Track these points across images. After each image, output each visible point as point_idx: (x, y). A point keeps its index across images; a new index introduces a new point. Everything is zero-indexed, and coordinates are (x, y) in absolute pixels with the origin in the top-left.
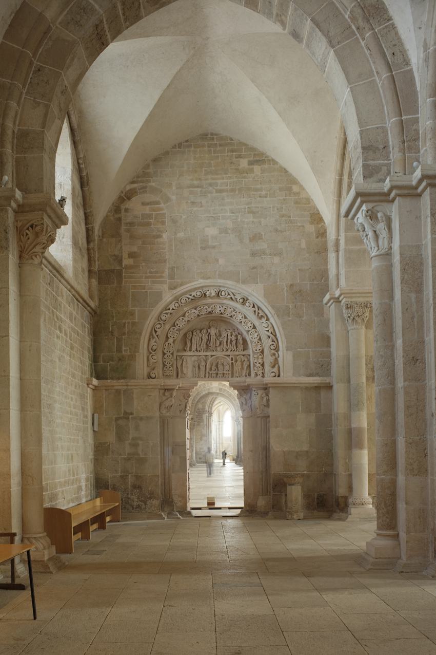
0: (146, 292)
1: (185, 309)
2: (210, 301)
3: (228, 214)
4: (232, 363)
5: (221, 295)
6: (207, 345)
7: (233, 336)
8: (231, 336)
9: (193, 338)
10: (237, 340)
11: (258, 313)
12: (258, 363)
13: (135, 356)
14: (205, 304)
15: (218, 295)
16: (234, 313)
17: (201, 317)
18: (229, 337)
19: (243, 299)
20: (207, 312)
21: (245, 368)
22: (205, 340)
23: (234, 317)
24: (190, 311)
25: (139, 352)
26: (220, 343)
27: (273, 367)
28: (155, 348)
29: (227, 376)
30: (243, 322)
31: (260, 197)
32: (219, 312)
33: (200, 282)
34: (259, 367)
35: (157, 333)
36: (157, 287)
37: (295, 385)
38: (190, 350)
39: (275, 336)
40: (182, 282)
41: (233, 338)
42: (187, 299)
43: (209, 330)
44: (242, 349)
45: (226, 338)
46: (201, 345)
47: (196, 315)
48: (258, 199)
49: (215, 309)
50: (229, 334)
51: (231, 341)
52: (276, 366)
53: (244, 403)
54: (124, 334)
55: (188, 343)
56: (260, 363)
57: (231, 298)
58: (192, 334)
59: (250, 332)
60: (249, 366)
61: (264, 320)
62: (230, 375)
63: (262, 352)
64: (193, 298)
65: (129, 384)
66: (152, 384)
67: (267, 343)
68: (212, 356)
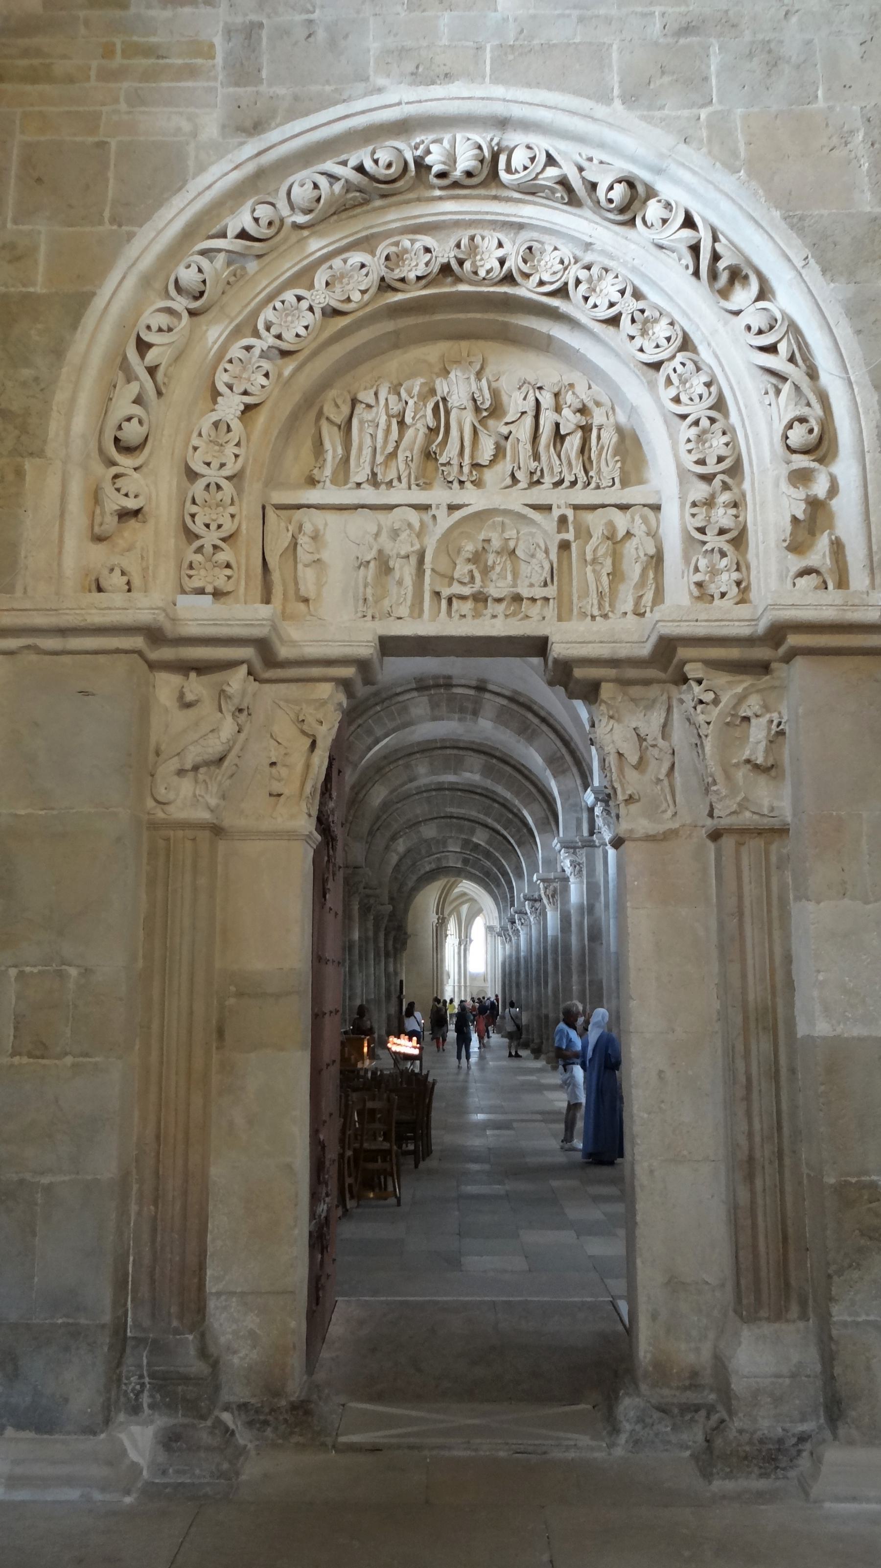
0: (102, 145)
4: (565, 546)
5: (508, 169)
6: (429, 455)
7: (566, 412)
8: (558, 409)
10: (586, 430)
11: (716, 257)
13: (20, 473)
16: (575, 271)
17: (399, 297)
18: (547, 419)
19: (631, 185)
20: (436, 269)
21: (634, 571)
22: (415, 435)
23: (577, 295)
24: (337, 262)
25: (39, 453)
26: (499, 452)
28: (132, 432)
29: (535, 611)
30: (625, 321)
32: (498, 273)
35: (152, 356)
39: (813, 374)
40: (296, 98)
41: (569, 420)
42: (323, 182)
43: (442, 387)
44: (617, 475)
45: (529, 420)
46: (393, 455)
47: (374, 278)
49: (473, 248)
50: (546, 400)
51: (559, 437)
52: (823, 542)
53: (633, 759)
55: (327, 445)
56: (722, 532)
57: (564, 182)
58: (354, 402)
59: (667, 369)
60: (657, 560)
61: (742, 297)
63: (736, 470)
66: (97, 618)
68: (452, 508)
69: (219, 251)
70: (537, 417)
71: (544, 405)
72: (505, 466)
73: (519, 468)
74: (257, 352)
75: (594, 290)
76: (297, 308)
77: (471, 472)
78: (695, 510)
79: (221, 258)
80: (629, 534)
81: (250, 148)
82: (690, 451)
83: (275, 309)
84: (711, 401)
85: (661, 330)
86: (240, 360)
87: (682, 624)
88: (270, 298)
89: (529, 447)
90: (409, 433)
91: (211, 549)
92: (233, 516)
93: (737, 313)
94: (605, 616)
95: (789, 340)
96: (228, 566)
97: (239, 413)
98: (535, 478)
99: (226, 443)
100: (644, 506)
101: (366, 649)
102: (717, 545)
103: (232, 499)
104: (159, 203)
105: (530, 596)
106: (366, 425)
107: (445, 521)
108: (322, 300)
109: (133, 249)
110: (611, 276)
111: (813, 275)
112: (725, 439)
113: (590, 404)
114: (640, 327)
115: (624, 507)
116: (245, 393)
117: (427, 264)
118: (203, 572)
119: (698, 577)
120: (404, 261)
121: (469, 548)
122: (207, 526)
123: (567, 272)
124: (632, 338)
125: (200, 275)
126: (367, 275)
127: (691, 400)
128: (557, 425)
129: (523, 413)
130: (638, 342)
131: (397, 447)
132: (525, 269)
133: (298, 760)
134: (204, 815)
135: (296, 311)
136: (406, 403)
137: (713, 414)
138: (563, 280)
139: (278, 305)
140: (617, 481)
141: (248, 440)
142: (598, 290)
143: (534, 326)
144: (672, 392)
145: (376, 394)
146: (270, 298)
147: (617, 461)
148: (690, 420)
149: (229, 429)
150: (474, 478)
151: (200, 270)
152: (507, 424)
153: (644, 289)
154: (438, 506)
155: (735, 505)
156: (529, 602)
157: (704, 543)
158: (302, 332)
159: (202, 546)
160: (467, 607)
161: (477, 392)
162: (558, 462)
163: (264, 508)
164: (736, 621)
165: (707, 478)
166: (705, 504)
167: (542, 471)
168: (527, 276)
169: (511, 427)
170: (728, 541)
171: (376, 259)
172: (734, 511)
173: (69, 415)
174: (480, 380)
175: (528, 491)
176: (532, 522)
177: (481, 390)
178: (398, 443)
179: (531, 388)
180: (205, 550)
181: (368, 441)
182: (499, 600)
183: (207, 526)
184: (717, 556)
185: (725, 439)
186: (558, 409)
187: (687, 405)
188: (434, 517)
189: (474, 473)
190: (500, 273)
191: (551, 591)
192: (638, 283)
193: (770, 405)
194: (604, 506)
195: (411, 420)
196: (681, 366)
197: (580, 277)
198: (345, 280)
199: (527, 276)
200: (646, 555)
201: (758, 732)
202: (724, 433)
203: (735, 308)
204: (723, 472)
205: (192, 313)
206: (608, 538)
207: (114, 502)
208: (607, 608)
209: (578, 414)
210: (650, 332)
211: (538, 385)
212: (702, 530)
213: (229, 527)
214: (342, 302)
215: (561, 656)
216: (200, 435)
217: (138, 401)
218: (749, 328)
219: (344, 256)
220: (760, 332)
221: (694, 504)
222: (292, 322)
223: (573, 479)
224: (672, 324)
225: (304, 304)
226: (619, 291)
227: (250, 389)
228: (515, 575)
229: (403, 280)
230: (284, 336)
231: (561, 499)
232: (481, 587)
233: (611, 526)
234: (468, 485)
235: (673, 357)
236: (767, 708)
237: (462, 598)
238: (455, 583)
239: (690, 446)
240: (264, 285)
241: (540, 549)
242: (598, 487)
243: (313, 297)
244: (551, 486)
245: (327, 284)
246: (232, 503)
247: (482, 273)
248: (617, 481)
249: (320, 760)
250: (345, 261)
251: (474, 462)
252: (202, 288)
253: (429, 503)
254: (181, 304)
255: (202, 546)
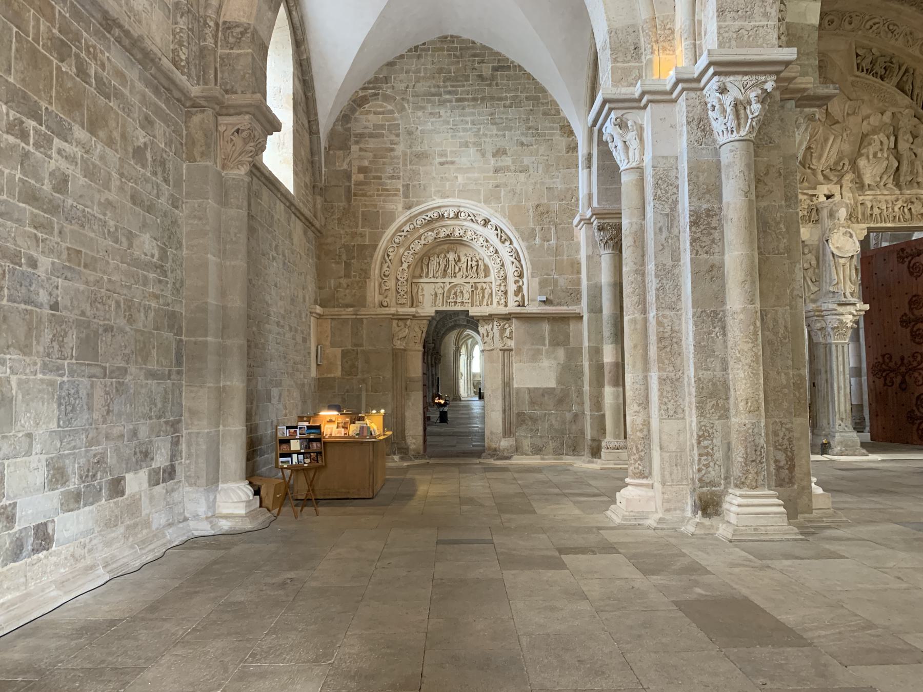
1: (422, 231)
2: (449, 222)
3: (470, 126)
4: (472, 291)
10: (478, 265)
11: (501, 236)
13: (366, 282)
14: (443, 226)
15: (457, 216)
18: (470, 263)
21: (486, 296)
22: (442, 266)
26: (460, 269)
27: (517, 295)
28: (387, 273)
31: (505, 107)
33: (438, 202)
36: (390, 206)
37: (542, 316)
38: (427, 276)
39: (519, 261)
41: (474, 264)
43: (448, 255)
48: (502, 109)
49: (454, 230)
50: (469, 259)
51: (472, 267)
54: (354, 257)
60: (491, 294)
61: (507, 243)
64: (429, 219)
65: (359, 313)
66: (384, 312)
67: (511, 270)
68: (450, 283)
72: (461, 273)
81: (409, 212)
104: (390, 225)
107: (448, 286)
109: (385, 235)
111: (520, 240)
133: (420, 335)
134: (402, 347)
173: (375, 270)
201: (508, 331)
207: (384, 288)
217: (388, 267)
231: (472, 281)
233: (482, 287)
236: (510, 326)
240: (411, 239)
249: (424, 335)
254: (395, 245)
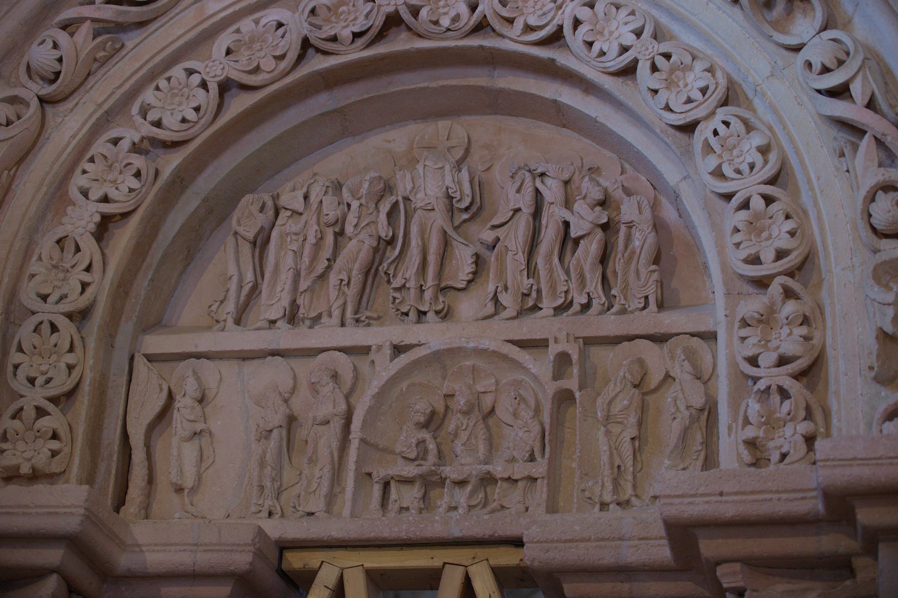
4: (565, 398)
7: (580, 206)
8: (568, 204)
9: (275, 234)
12: (767, 359)
20: (379, 21)
23: (575, 40)
24: (246, 25)
29: (514, 498)
30: (643, 68)
32: (468, 20)
34: (784, 394)
44: (651, 290)
45: (523, 223)
46: (323, 277)
50: (551, 190)
59: (704, 132)
62: (542, 489)
68: (398, 350)
69: (81, 20)
70: (537, 214)
71: (548, 195)
73: (506, 288)
74: (125, 145)
75: (601, 33)
76: (187, 86)
77: (436, 298)
78: (744, 332)
79: (85, 29)
80: (668, 377)
82: (737, 245)
83: (157, 88)
84: (768, 171)
85: (696, 79)
86: (105, 157)
87: (697, 500)
88: (152, 76)
89: (522, 258)
90: (351, 246)
91: (33, 413)
92: (70, 368)
93: (797, 49)
94: (624, 504)
95: (865, 78)
96: (55, 436)
97: (92, 227)
98: (530, 303)
99: (73, 267)
100: (693, 335)
101: (242, 560)
102: (775, 382)
103: (72, 343)
105: (506, 476)
106: (289, 239)
108: (219, 72)
110: (623, 13)
112: (789, 225)
113: (618, 194)
114: (664, 77)
115: (659, 339)
116: (105, 199)
117: (367, 16)
118: (21, 445)
119: (750, 432)
120: (338, 15)
121: (421, 407)
122: (32, 381)
123: (560, 12)
124: (656, 92)
125: (55, 52)
126: (283, 37)
127: (738, 172)
128: (567, 224)
129: (518, 210)
130: (663, 96)
131: (329, 268)
132: (505, 13)
135: (185, 90)
136: (349, 205)
137: (769, 190)
138: (555, 22)
139: (163, 83)
140: (652, 300)
141: (105, 264)
142: (606, 32)
143: (534, 91)
144: (712, 162)
145: (306, 197)
146: (152, 76)
147: (654, 271)
148: (736, 201)
149: (78, 249)
150: (440, 307)
151: (55, 46)
152: (495, 227)
153: (675, 27)
154: (380, 348)
155: (806, 321)
156: (505, 485)
157: (756, 380)
158: (191, 115)
159: (22, 409)
160: (410, 496)
161: (452, 185)
162: (563, 277)
163: (132, 359)
164: (782, 492)
165: (762, 283)
166: (760, 321)
167: (539, 291)
168: (511, 21)
169: (500, 232)
170: (798, 376)
171: (297, 15)
172: (804, 330)
174: (460, 171)
175: (516, 322)
176: (517, 365)
177: (459, 183)
178: (331, 260)
179: (527, 174)
180: (24, 413)
181: (289, 261)
182: (462, 483)
183: (32, 381)
184: (776, 398)
185: (789, 225)
186: (568, 204)
187: (733, 179)
188: (373, 362)
189: (441, 299)
190: (469, 20)
191: (539, 468)
192: (664, 20)
193: (848, 171)
194: (631, 338)
195: (352, 229)
196: (724, 126)
197: (579, 17)
198: (257, 46)
199: (511, 21)
200: (688, 407)
202: (788, 217)
203: (793, 41)
204: (790, 274)
205: (42, 100)
206: (635, 386)
208: (630, 491)
209: (598, 209)
210: (681, 83)
211: (539, 170)
212: (753, 361)
213: (61, 383)
214: (250, 72)
215: (536, 564)
216: (40, 259)
218: (809, 65)
219: (256, 16)
220: (826, 70)
221: (745, 323)
222: (180, 104)
223: (584, 301)
224: (710, 70)
225: (196, 79)
226: (633, 32)
227: (113, 194)
228: (491, 445)
229: (334, 39)
230: (165, 122)
232: (434, 465)
234: (431, 316)
235: (713, 113)
237: (407, 481)
238: (400, 461)
239: (738, 238)
241: (528, 406)
242: (623, 311)
243: (208, 70)
244: (552, 312)
245: (229, 52)
246: (71, 349)
247: (445, 22)
248: (652, 300)
250: (257, 22)
251: (443, 285)
252: (57, 67)
253: (369, 343)
254: (33, 90)
255: (22, 409)
